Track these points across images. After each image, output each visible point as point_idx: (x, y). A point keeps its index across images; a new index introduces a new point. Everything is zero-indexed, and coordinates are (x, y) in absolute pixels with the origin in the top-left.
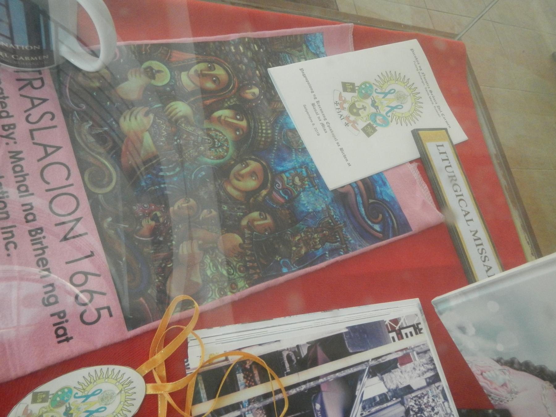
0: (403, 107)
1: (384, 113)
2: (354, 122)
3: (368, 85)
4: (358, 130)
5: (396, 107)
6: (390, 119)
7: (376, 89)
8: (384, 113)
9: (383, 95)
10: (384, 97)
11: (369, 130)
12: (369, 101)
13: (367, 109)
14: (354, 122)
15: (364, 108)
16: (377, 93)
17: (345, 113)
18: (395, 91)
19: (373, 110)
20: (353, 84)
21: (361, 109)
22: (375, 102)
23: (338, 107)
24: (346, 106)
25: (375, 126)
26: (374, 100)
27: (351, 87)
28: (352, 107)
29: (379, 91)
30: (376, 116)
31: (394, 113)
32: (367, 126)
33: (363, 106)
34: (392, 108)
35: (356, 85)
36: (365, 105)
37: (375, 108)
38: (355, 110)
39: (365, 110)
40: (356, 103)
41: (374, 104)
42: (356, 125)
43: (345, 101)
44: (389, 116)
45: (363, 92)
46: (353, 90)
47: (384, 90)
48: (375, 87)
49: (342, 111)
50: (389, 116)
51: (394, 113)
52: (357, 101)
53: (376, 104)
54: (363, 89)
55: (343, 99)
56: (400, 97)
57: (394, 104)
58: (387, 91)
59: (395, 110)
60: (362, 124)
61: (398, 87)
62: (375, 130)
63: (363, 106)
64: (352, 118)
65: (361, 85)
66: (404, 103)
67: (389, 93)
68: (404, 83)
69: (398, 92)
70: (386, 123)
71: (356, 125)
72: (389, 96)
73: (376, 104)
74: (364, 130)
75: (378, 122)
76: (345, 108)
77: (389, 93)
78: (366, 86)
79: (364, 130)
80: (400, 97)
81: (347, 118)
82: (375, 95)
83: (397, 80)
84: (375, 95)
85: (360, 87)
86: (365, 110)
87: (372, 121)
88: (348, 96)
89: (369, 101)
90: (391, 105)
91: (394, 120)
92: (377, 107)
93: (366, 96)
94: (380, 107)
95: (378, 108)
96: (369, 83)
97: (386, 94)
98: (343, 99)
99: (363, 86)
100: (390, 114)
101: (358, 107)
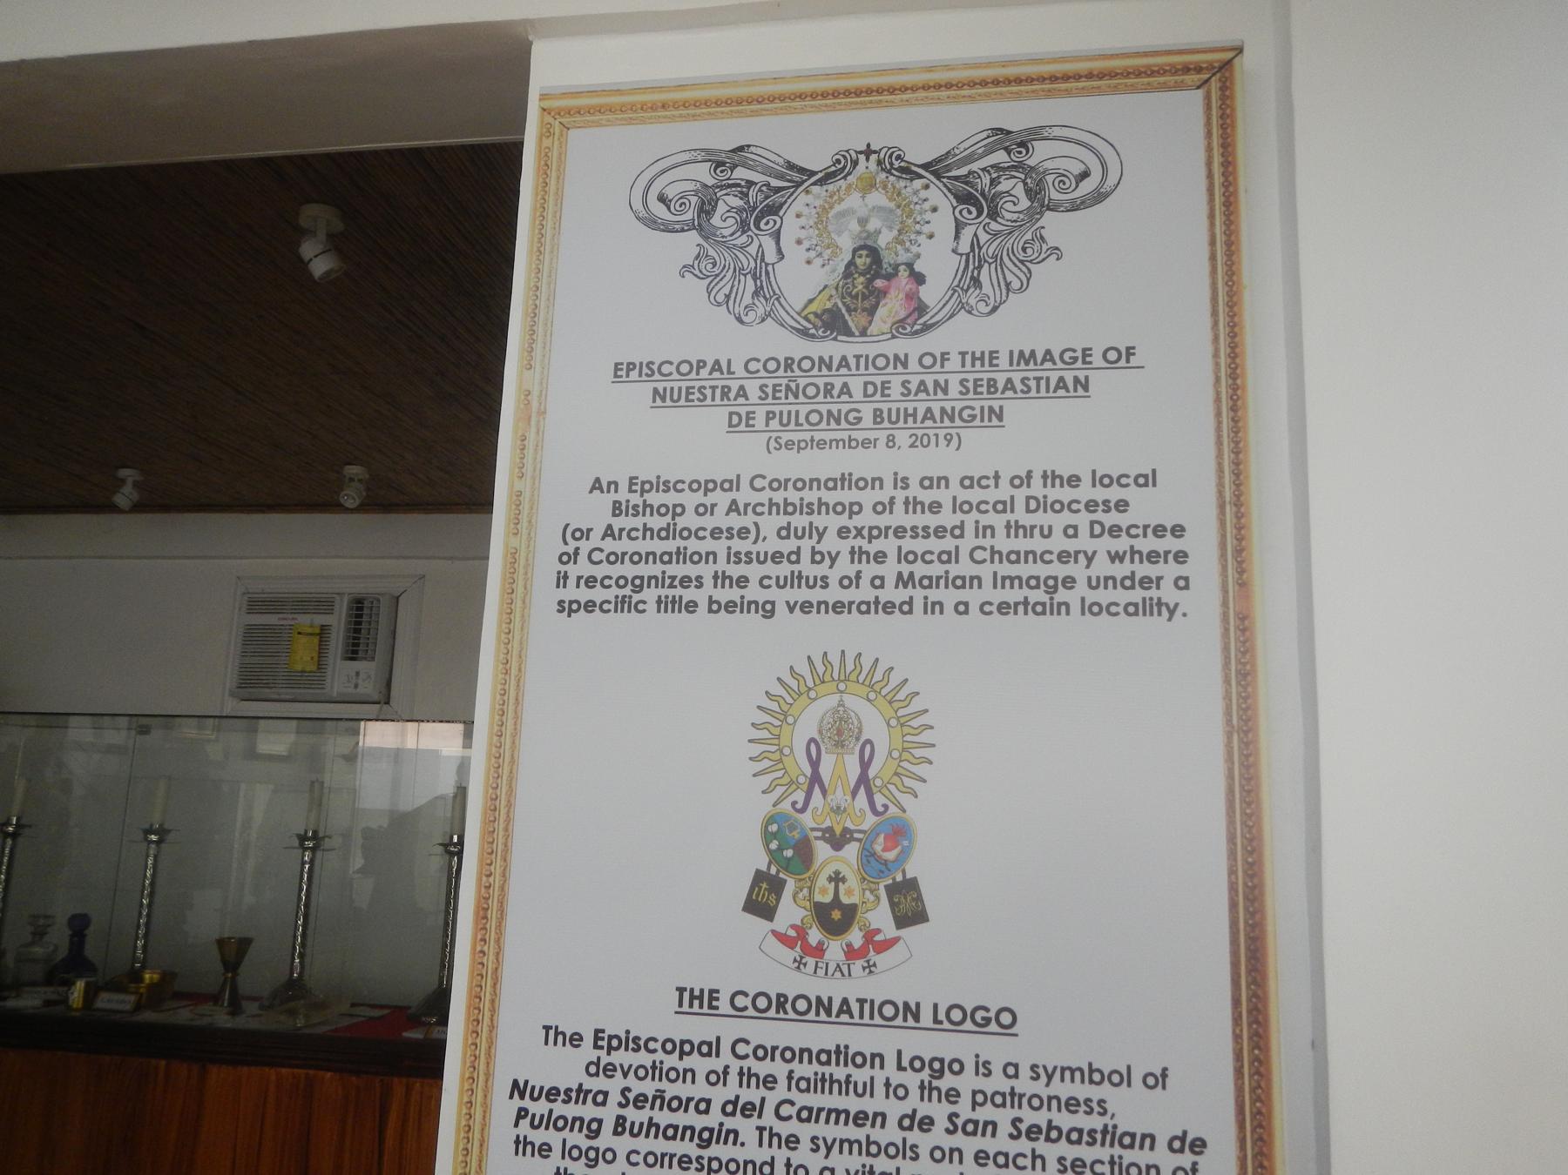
0: (868, 741)
1: (870, 821)
2: (870, 935)
3: (774, 828)
4: (895, 941)
5: (865, 765)
7: (794, 804)
8: (870, 821)
9: (817, 790)
10: (824, 792)
11: (909, 907)
13: (846, 871)
14: (870, 935)
15: (837, 879)
16: (803, 810)
17: (835, 951)
18: (812, 740)
19: (851, 851)
20: (760, 877)
21: (837, 888)
22: (830, 830)
25: (899, 878)
26: (824, 831)
27: (764, 886)
28: (822, 914)
29: (800, 797)
30: (874, 854)
32: (893, 905)
33: (830, 879)
34: (863, 780)
35: (764, 869)
36: (829, 871)
38: (836, 915)
39: (844, 880)
40: (818, 898)
41: (838, 841)
42: (878, 938)
43: (801, 932)
45: (789, 853)
46: (777, 886)
47: (802, 779)
48: (786, 806)
49: (827, 956)
50: (886, 807)
51: (878, 782)
53: (838, 831)
54: (780, 849)
55: (792, 933)
56: (841, 731)
57: (854, 771)
58: (808, 771)
59: (872, 773)
60: (880, 917)
61: (808, 722)
62: (911, 885)
63: (830, 879)
64: (855, 937)
65: (770, 852)
66: (860, 732)
67: (815, 764)
68: (800, 694)
69: (820, 732)
70: (899, 833)
71: (878, 938)
72: (825, 770)
73: (838, 831)
74: (902, 921)
75: (890, 856)
76: (820, 943)
78: (774, 835)
79: (902, 921)
80: (841, 731)
81: (851, 953)
82: (807, 820)
83: (785, 714)
84: (807, 820)
85: (774, 856)
86: (844, 880)
87: (881, 874)
88: (790, 912)
89: (822, 850)
92: (846, 830)
93: (804, 852)
94: (849, 825)
96: (770, 820)
97: (816, 779)
98: (792, 933)
99: (774, 845)
100: (879, 800)
101: (828, 899)
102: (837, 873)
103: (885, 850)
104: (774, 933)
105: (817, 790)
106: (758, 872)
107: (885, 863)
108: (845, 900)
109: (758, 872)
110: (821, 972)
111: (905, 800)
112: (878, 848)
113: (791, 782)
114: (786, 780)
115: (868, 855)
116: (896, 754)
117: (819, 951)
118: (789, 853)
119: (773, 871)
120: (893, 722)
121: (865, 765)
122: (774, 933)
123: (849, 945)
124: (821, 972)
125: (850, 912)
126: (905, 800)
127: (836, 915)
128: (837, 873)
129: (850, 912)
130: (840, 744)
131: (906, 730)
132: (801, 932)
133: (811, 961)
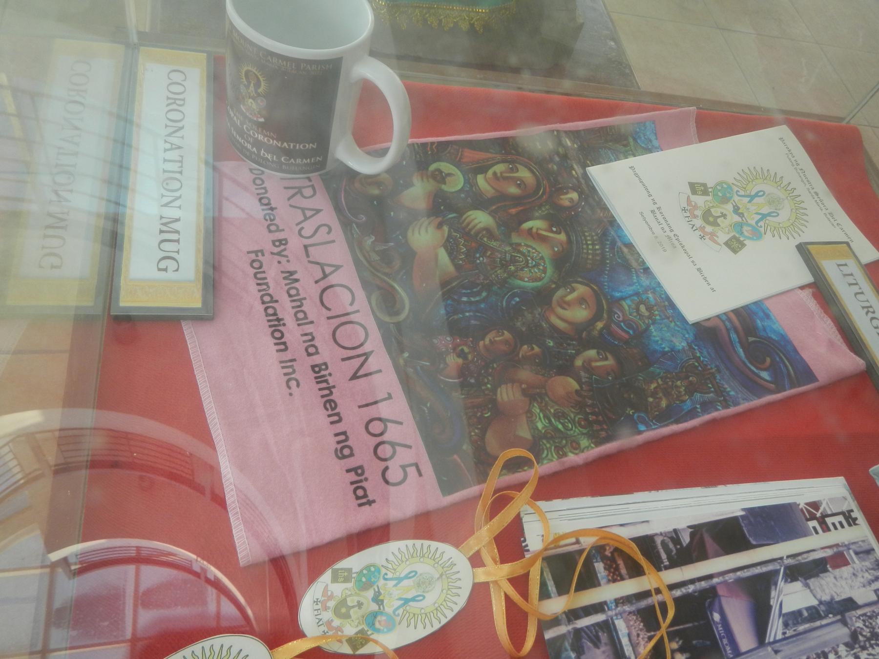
0: (424, 597)
3: (372, 569)
5: (413, 599)
6: (398, 619)
7: (386, 574)
10: (395, 585)
12: (370, 594)
13: (364, 607)
14: (339, 629)
16: (386, 579)
18: (416, 573)
19: (374, 607)
21: (353, 607)
23: (319, 606)
24: (331, 604)
26: (379, 592)
30: (375, 617)
31: (408, 608)
33: (358, 602)
36: (362, 600)
37: (378, 604)
39: (360, 608)
40: (348, 599)
43: (331, 597)
44: (398, 615)
45: (364, 580)
46: (347, 580)
47: (398, 574)
52: (350, 595)
53: (381, 598)
54: (364, 575)
55: (329, 593)
57: (409, 596)
58: (402, 576)
59: (411, 603)
63: (358, 602)
65: (361, 571)
67: (407, 577)
73: (381, 598)
76: (329, 608)
77: (407, 577)
78: (369, 571)
83: (423, 556)
84: (381, 582)
86: (360, 608)
87: (368, 625)
89: (370, 594)
90: (404, 597)
91: (405, 621)
92: (382, 601)
93: (366, 586)
94: (385, 602)
95: (382, 604)
97: (400, 580)
98: (329, 593)
100: (400, 611)
101: (350, 604)
102: (362, 604)
103: (379, 621)
104: (327, 585)
105: (394, 582)
106: (351, 569)
107: (374, 624)
108: (352, 612)
109: (351, 569)
110: (316, 613)
111: (405, 623)
112: (379, 618)
113: (395, 570)
114: (395, 567)
115: (374, 615)
116: (423, 611)
117: (326, 608)
118: (364, 580)
119: (354, 575)
120: (436, 605)
121: (413, 599)
122: (327, 585)
123: (332, 621)
124: (316, 613)
125: (347, 616)
126: (405, 623)
127: (343, 610)
128: (362, 604)
129: (347, 616)
130: (419, 585)
131: (435, 612)
132: (331, 597)
133: (319, 606)
